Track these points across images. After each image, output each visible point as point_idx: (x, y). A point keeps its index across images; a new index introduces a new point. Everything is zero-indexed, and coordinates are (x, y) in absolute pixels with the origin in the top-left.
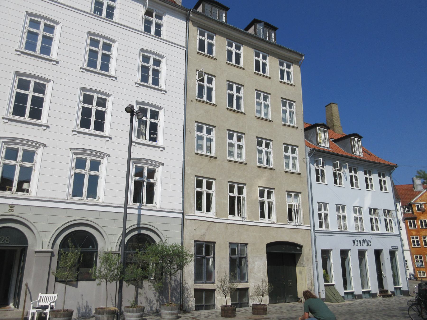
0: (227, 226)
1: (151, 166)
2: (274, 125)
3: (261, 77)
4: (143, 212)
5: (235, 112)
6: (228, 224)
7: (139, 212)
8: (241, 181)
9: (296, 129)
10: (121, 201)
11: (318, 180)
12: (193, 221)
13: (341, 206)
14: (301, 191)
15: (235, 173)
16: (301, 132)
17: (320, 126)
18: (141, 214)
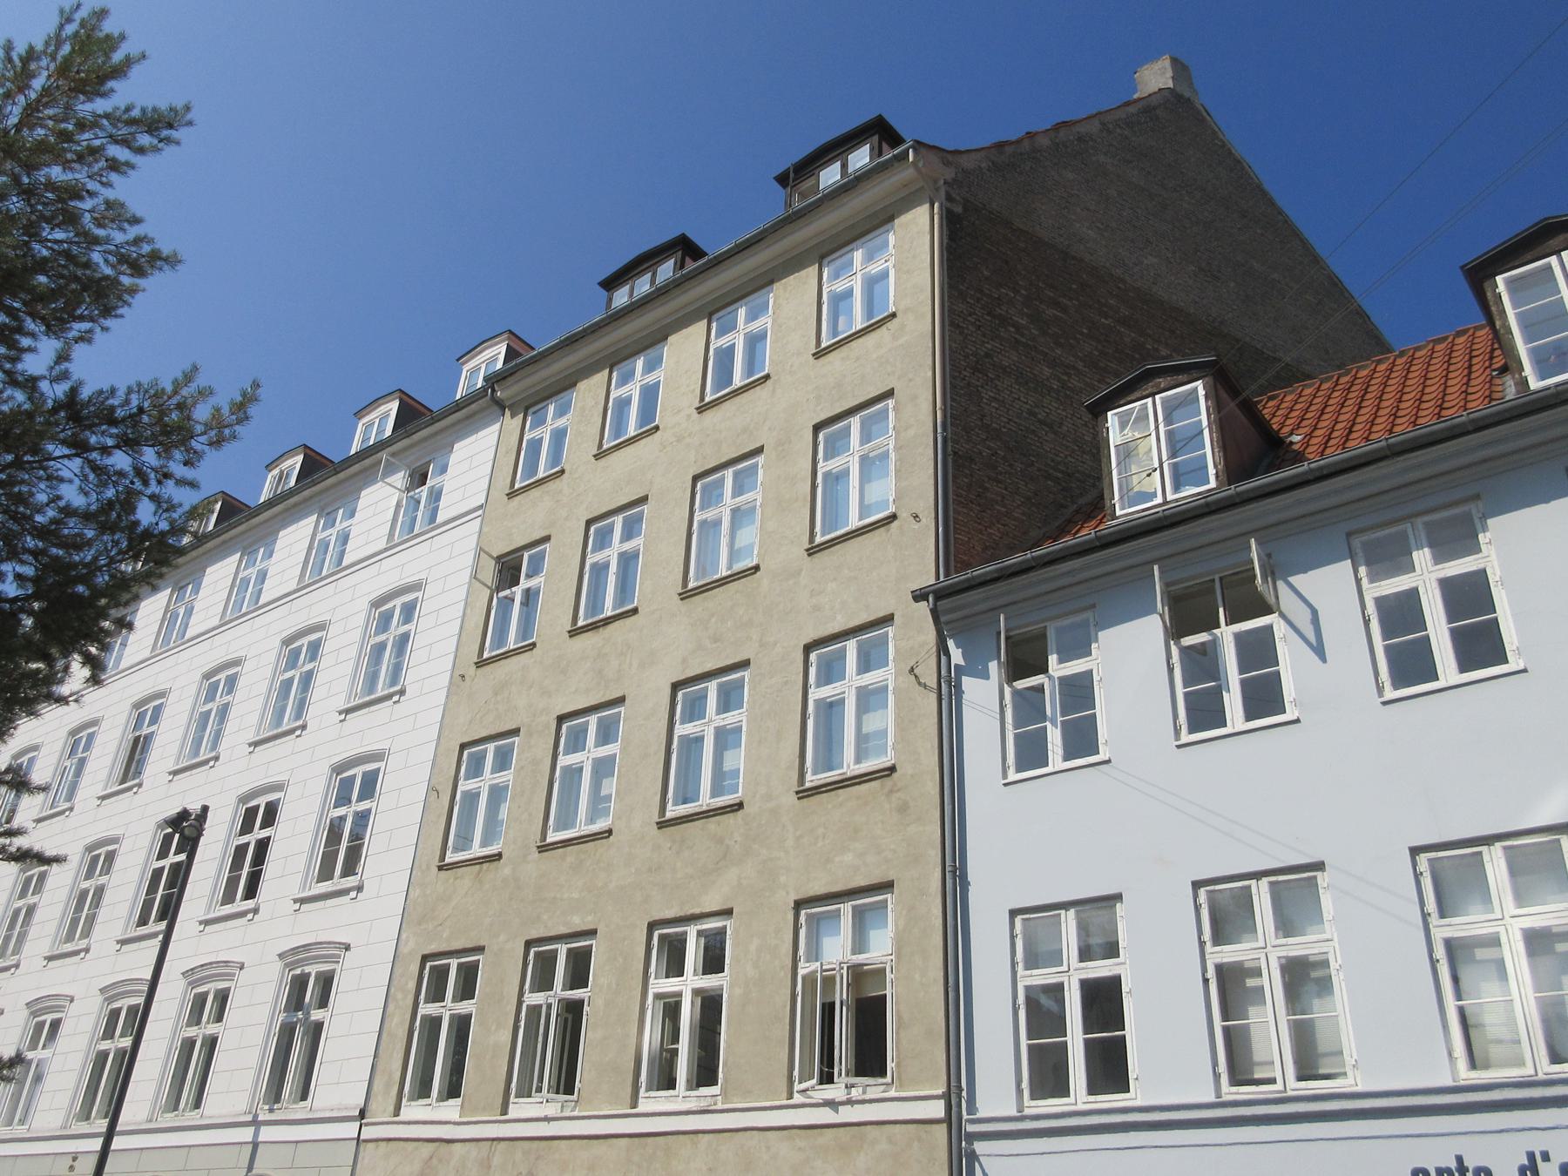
0: (491, 1154)
1: (325, 965)
2: (765, 582)
3: (727, 406)
4: (267, 1134)
5: (599, 627)
6: (495, 1143)
7: (256, 1134)
8: (578, 922)
9: (888, 530)
10: (234, 1106)
11: (1031, 753)
12: (384, 1144)
13: (1265, 881)
14: (891, 875)
15: (558, 896)
16: (916, 526)
17: (1137, 394)
18: (260, 1139)
